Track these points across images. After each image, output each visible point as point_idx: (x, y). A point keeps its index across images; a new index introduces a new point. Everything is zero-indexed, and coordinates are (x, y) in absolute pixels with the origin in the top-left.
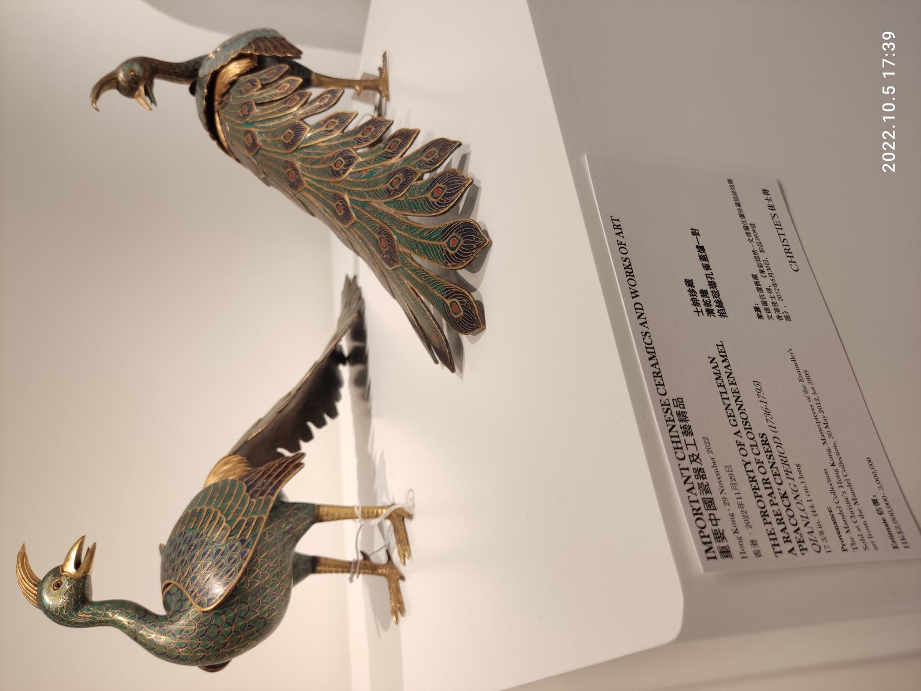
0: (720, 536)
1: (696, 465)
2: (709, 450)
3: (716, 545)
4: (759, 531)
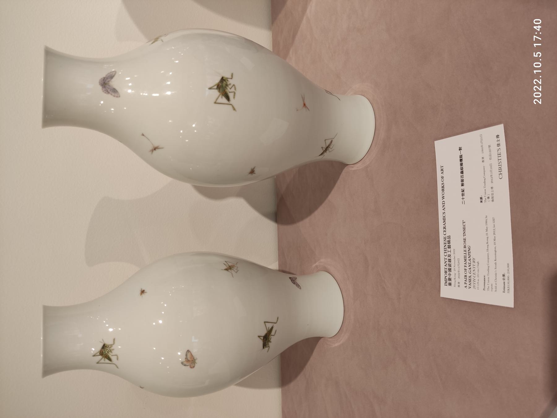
0: (450, 279)
1: (449, 258)
2: (454, 253)
3: (448, 282)
4: (462, 280)
